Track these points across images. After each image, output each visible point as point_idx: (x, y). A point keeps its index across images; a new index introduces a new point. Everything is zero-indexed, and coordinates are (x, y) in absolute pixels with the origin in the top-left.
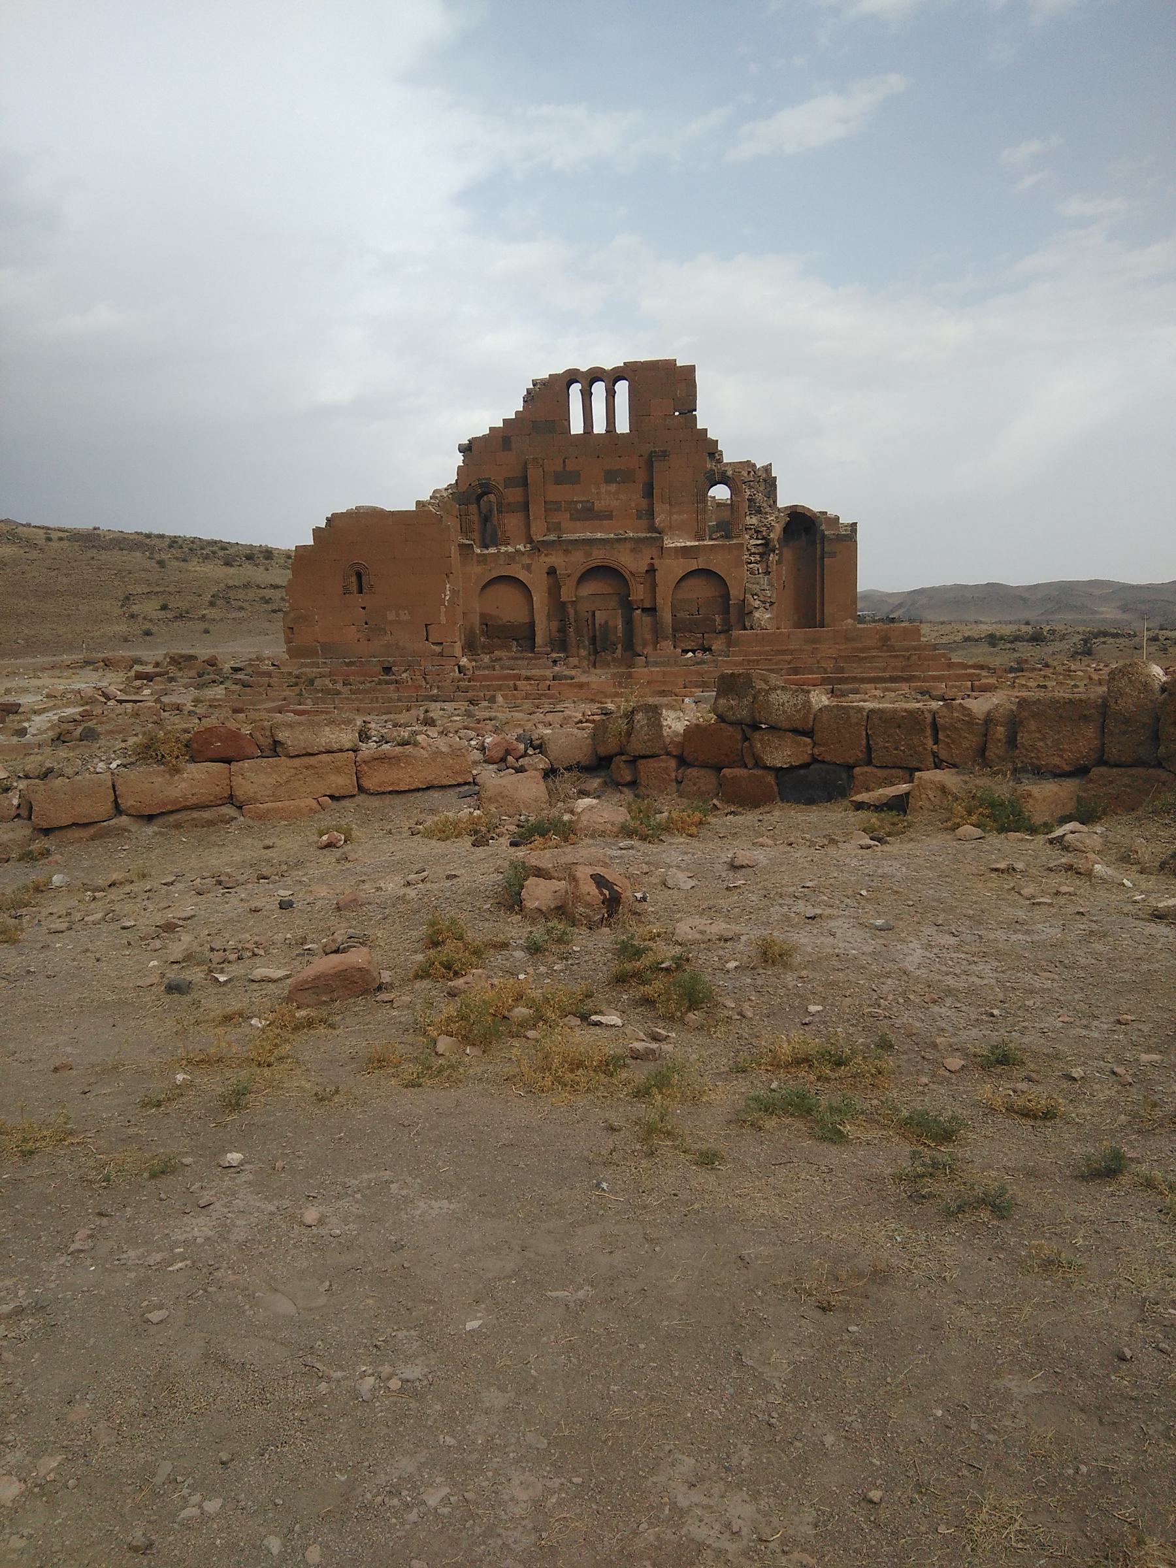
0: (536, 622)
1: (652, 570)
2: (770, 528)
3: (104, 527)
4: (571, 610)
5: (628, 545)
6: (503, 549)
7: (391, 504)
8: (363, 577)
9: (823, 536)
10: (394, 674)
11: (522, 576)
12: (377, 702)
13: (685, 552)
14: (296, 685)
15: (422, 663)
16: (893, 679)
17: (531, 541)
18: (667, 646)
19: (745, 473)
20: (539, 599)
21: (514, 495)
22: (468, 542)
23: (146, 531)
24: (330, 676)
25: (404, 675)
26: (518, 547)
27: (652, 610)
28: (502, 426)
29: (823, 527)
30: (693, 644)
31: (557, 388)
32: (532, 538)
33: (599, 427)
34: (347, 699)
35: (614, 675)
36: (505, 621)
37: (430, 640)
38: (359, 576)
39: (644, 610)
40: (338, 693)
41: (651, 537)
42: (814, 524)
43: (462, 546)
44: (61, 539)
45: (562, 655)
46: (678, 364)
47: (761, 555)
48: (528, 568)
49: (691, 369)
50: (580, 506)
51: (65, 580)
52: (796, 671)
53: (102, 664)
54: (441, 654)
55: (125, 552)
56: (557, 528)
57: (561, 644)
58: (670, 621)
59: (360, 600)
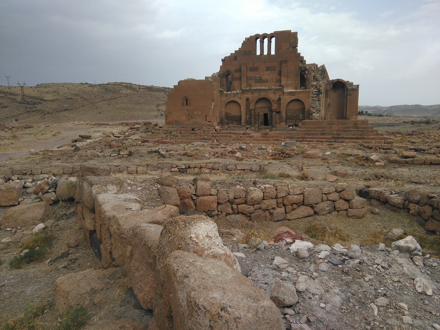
0: (242, 116)
1: (279, 99)
2: (320, 86)
3: (154, 85)
4: (253, 112)
5: (272, 91)
6: (233, 92)
7: (197, 78)
8: (188, 101)
9: (347, 89)
11: (238, 101)
12: (188, 139)
13: (291, 93)
14: (166, 133)
15: (204, 128)
16: (357, 138)
17: (242, 90)
18: (283, 124)
19: (313, 68)
20: (243, 108)
21: (237, 75)
22: (222, 90)
23: (165, 87)
24: (176, 131)
25: (198, 131)
26: (237, 91)
28: (234, 53)
29: (348, 86)
33: (266, 53)
34: (180, 138)
35: (262, 134)
36: (232, 115)
38: (187, 100)
39: (277, 112)
41: (280, 89)
42: (345, 85)
43: (220, 91)
44: (143, 88)
45: (249, 126)
46: (292, 32)
47: (317, 95)
49: (296, 33)
50: (258, 78)
51: (142, 100)
52: (323, 134)
53: (125, 124)
54: (209, 125)
55: (159, 92)
57: (249, 122)
58: (285, 116)
59: (187, 107)
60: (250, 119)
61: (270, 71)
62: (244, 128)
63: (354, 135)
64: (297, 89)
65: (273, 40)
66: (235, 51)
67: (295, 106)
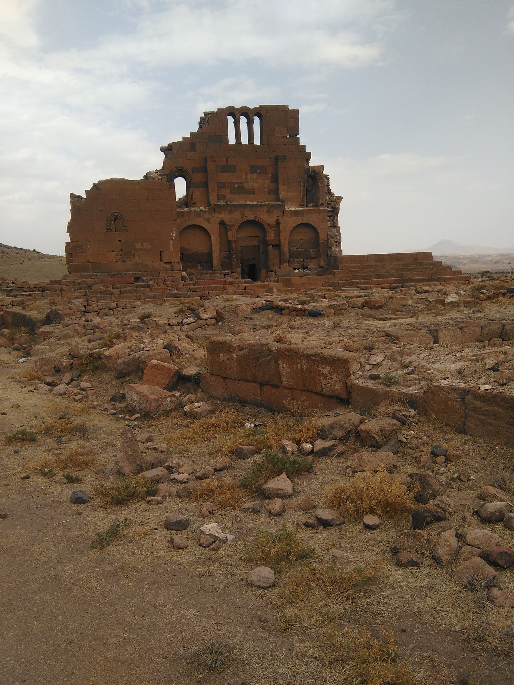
0: (214, 252)
4: (234, 245)
5: (265, 209)
6: (193, 209)
10: (144, 281)
11: (205, 225)
14: (81, 289)
17: (209, 205)
18: (286, 265)
20: (215, 239)
21: (198, 177)
24: (101, 283)
25: (151, 282)
26: (201, 208)
27: (278, 246)
30: (299, 265)
31: (223, 117)
32: (210, 203)
34: (120, 296)
37: (165, 260)
39: (273, 246)
40: (112, 293)
41: (279, 204)
46: (290, 108)
47: (330, 216)
48: (208, 220)
50: (236, 186)
52: (379, 276)
56: (223, 197)
57: (227, 264)
60: (227, 260)
61: (258, 173)
62: (218, 275)
63: (423, 275)
64: (304, 207)
65: (257, 121)
66: (191, 134)
67: (303, 236)
